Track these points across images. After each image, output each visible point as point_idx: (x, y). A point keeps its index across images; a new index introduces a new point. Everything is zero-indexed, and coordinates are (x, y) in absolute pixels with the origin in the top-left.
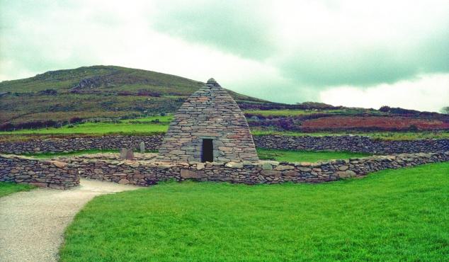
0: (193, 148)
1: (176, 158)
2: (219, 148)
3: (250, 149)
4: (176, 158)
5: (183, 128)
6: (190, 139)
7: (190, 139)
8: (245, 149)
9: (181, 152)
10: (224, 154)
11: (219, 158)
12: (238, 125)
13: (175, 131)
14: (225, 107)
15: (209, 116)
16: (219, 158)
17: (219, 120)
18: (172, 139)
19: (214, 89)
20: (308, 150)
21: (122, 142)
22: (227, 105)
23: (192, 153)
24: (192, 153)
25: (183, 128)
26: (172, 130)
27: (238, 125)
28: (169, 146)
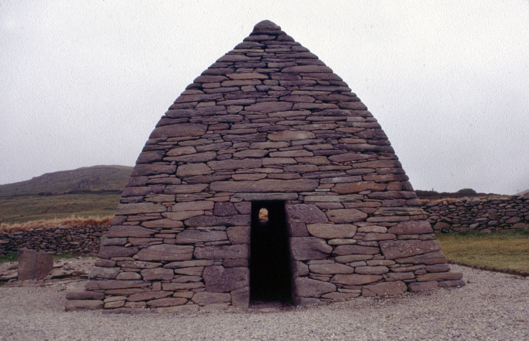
0: (217, 236)
1: (158, 272)
2: (312, 229)
3: (412, 225)
4: (158, 272)
5: (182, 170)
6: (209, 204)
7: (209, 204)
8: (399, 229)
9: (178, 252)
10: (329, 249)
11: (314, 265)
12: (365, 151)
13: (155, 179)
14: (316, 98)
15: (266, 126)
16: (314, 265)
17: (302, 135)
18: (143, 207)
19: (276, 47)
20: (462, 229)
21: (69, 237)
22: (321, 92)
23: (218, 252)
24: (218, 252)
25: (182, 170)
26: (144, 179)
27: (365, 151)
28: (133, 230)
